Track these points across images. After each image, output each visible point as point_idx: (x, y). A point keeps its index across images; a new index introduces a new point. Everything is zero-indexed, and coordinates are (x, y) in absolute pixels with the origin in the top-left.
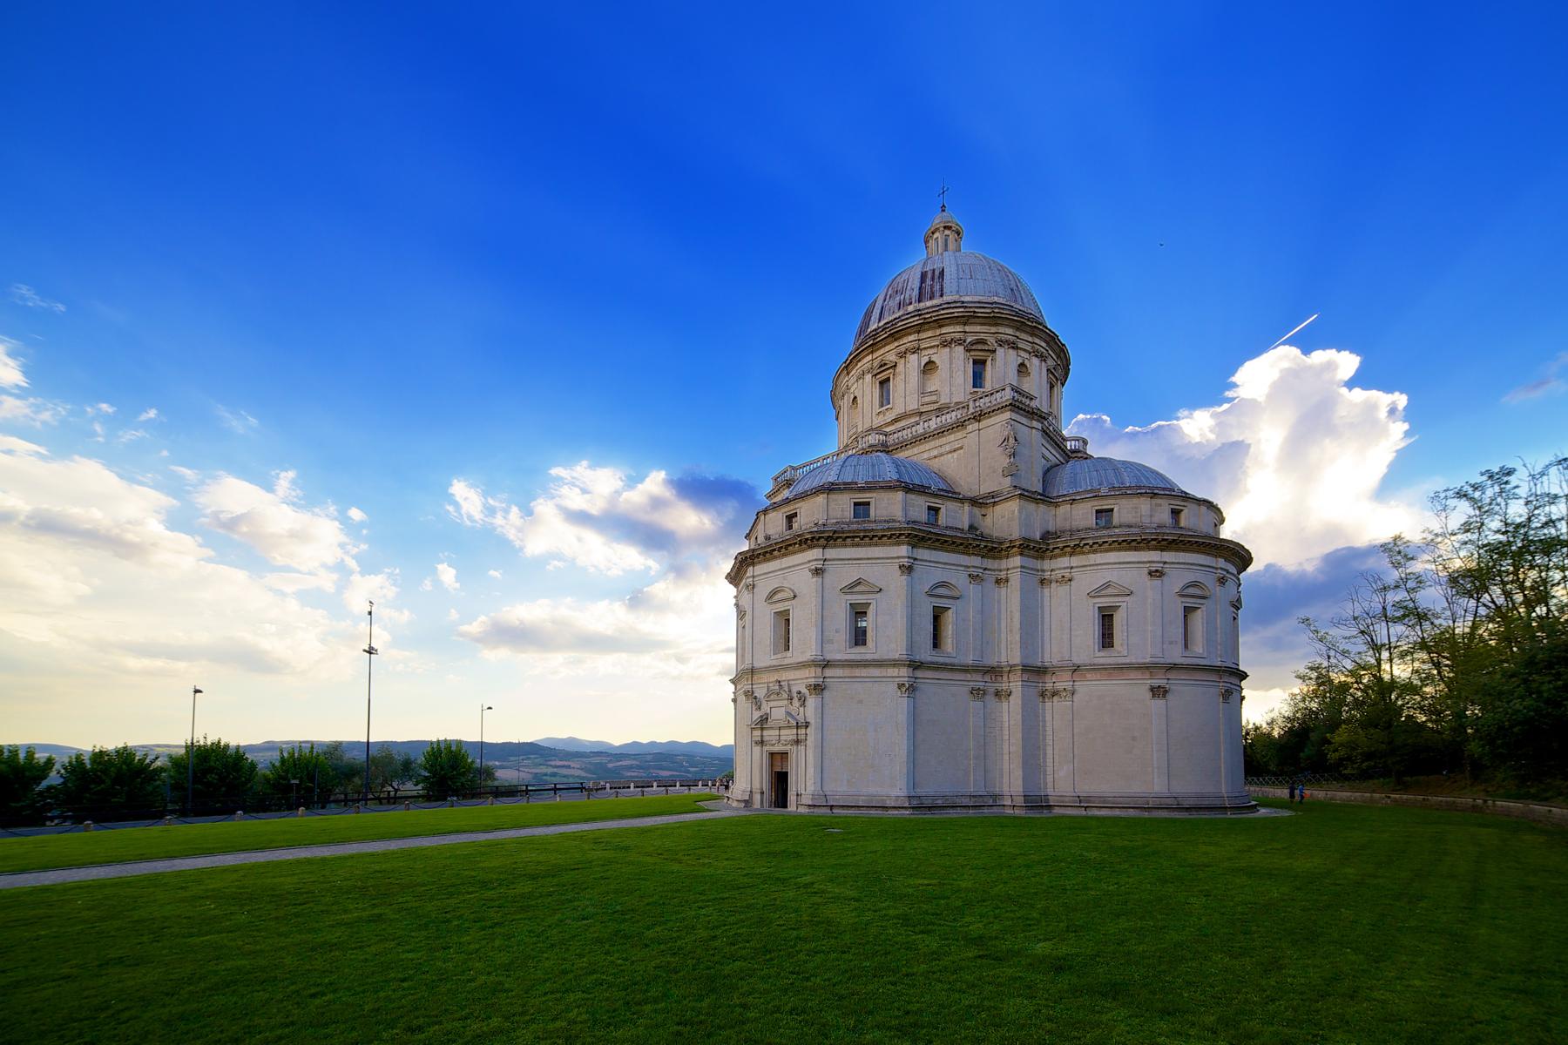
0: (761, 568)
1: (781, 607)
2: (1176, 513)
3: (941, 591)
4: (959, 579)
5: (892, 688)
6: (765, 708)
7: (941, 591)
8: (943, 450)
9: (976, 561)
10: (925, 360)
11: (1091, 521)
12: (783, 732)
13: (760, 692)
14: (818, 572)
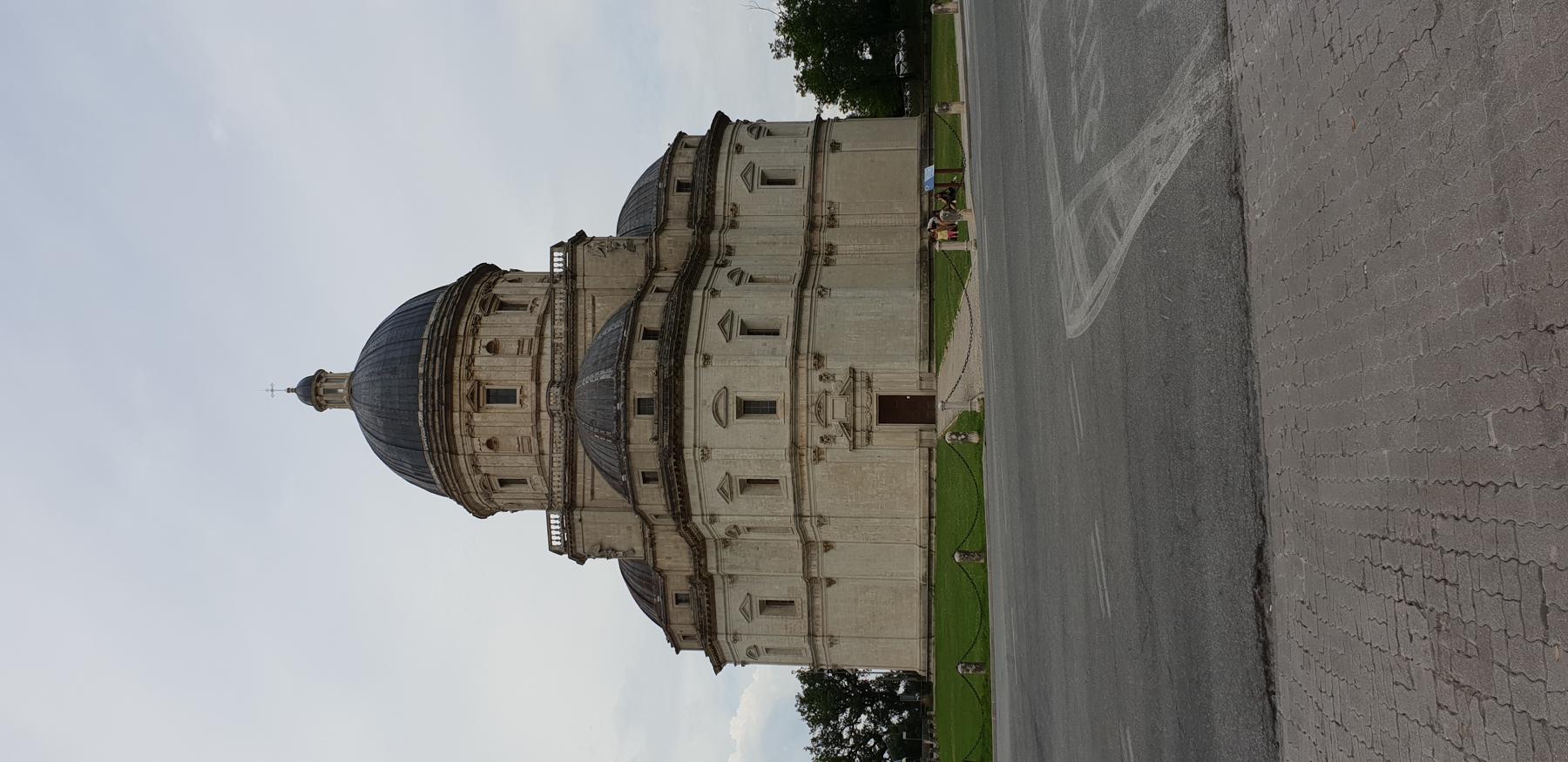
0: (688, 441)
1: (733, 409)
2: (687, 146)
3: (736, 278)
4: (728, 270)
5: (820, 302)
6: (835, 428)
7: (736, 278)
8: (589, 316)
9: (711, 263)
10: (484, 351)
11: (686, 195)
12: (858, 403)
13: (818, 431)
14: (707, 358)
